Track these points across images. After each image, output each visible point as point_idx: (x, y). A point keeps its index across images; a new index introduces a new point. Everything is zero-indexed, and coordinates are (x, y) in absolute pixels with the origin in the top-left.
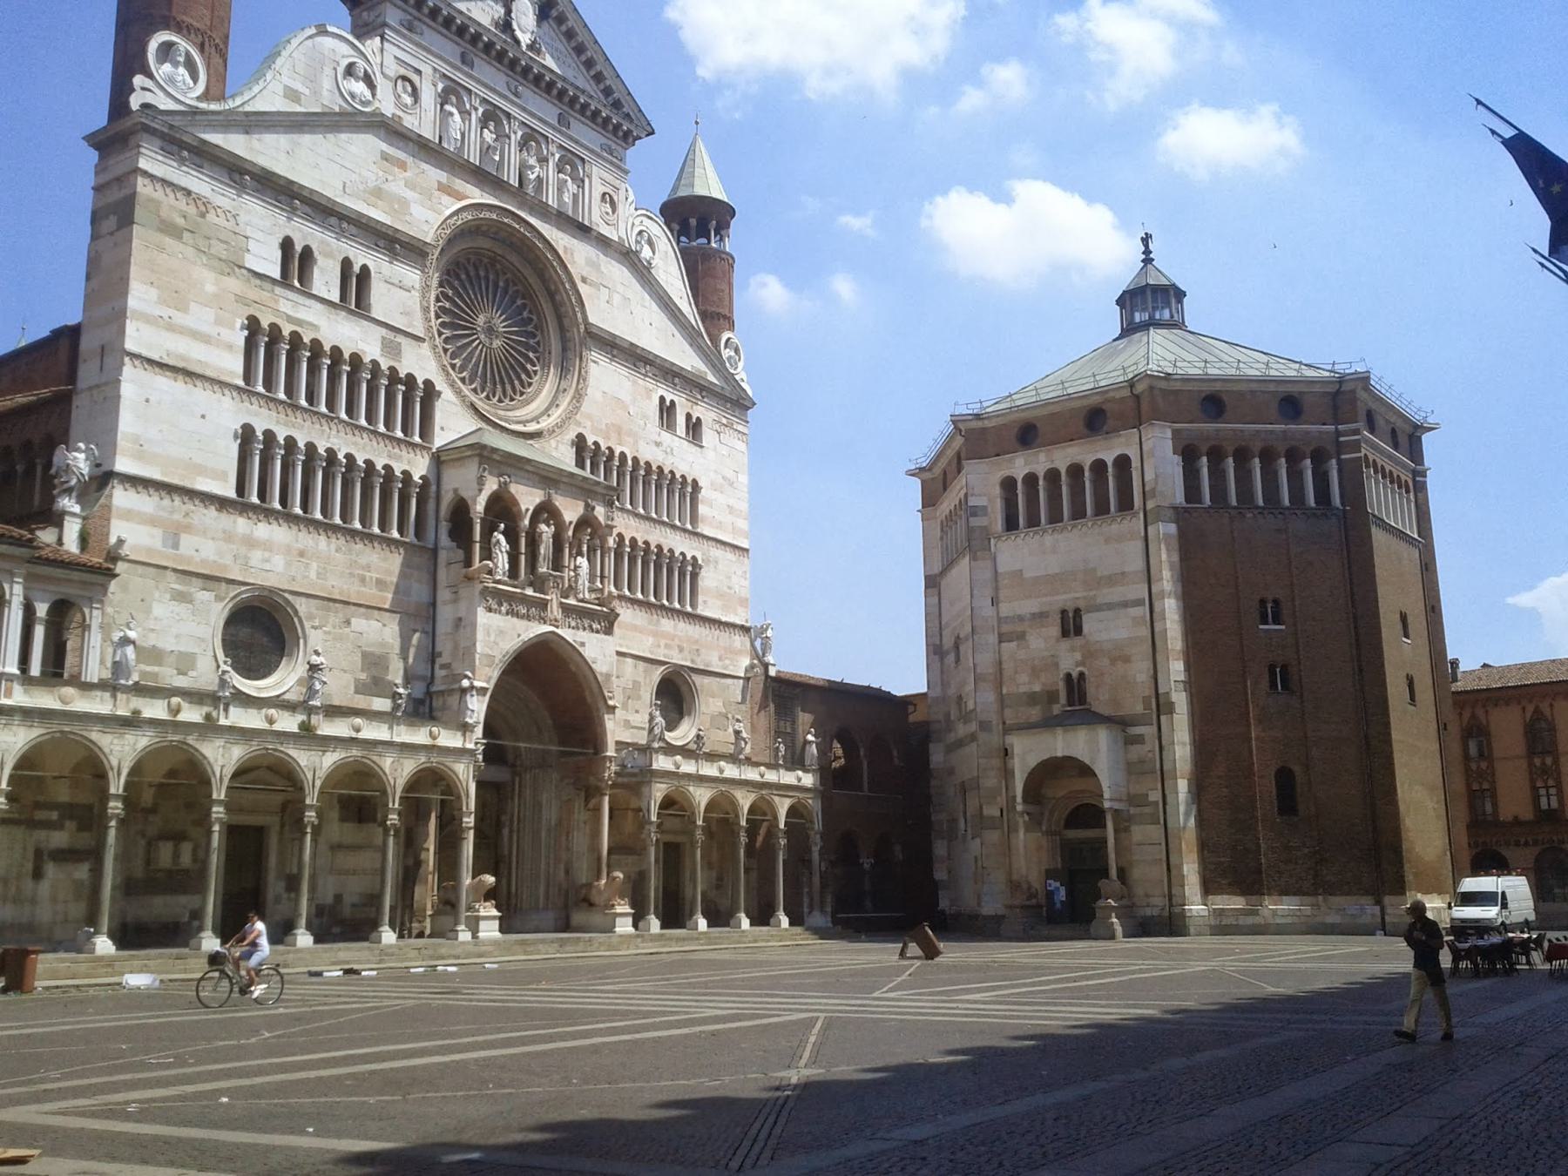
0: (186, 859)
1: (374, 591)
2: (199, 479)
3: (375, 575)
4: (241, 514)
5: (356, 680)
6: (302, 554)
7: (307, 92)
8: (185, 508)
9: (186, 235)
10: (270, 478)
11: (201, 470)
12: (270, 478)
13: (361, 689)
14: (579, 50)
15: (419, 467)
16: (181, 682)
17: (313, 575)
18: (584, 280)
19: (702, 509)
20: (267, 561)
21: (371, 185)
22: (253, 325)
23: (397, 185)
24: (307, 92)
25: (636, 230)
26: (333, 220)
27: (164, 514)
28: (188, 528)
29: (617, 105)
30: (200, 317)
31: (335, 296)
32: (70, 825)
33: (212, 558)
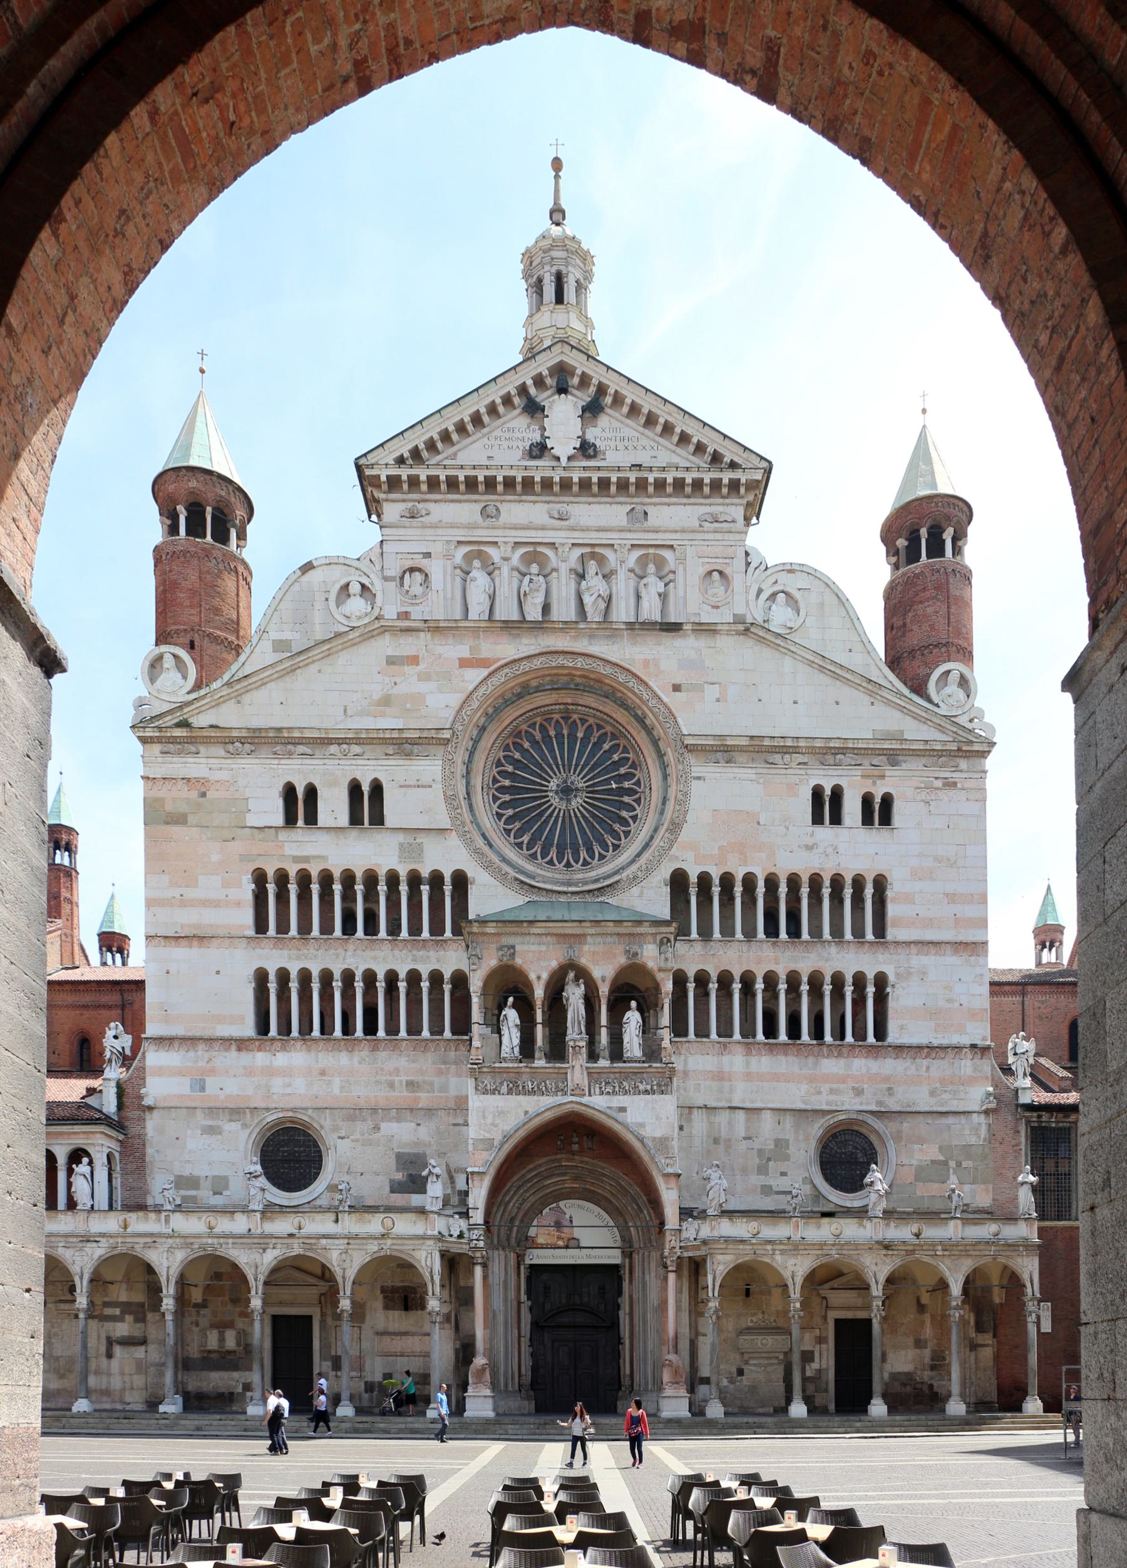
0: (231, 1343)
1: (405, 1094)
2: (219, 1027)
3: (404, 1079)
4: (259, 1050)
5: (391, 1181)
6: (323, 1073)
7: (297, 636)
8: (207, 1055)
9: (190, 818)
10: (282, 1010)
11: (220, 1019)
12: (282, 1010)
13: (397, 1188)
14: (650, 420)
15: (449, 959)
16: (218, 1201)
17: (336, 1091)
18: (677, 688)
19: (891, 910)
20: (290, 1085)
21: (376, 697)
22: (260, 878)
23: (409, 682)
24: (297, 636)
25: (764, 596)
26: (333, 749)
27: (189, 1064)
28: (213, 1072)
29: (716, 458)
30: (209, 886)
31: (344, 819)
32: (129, 1318)
33: (235, 1092)
